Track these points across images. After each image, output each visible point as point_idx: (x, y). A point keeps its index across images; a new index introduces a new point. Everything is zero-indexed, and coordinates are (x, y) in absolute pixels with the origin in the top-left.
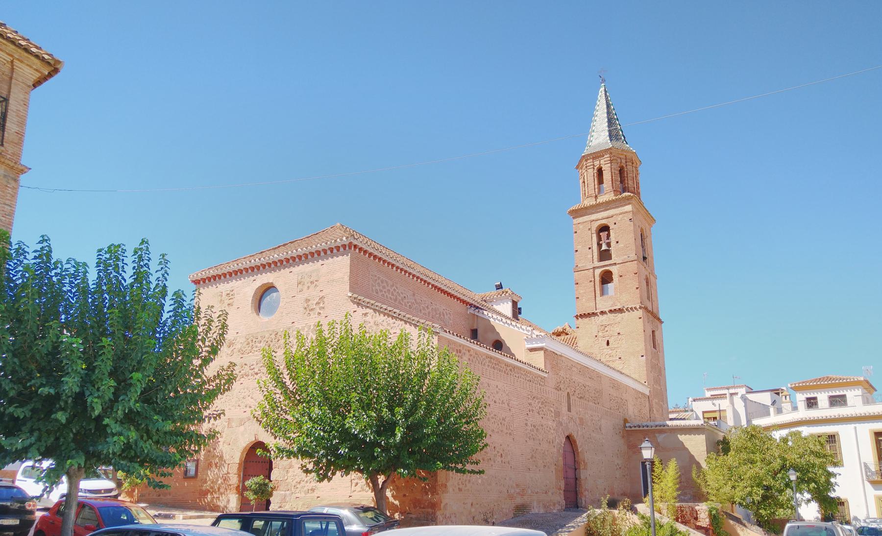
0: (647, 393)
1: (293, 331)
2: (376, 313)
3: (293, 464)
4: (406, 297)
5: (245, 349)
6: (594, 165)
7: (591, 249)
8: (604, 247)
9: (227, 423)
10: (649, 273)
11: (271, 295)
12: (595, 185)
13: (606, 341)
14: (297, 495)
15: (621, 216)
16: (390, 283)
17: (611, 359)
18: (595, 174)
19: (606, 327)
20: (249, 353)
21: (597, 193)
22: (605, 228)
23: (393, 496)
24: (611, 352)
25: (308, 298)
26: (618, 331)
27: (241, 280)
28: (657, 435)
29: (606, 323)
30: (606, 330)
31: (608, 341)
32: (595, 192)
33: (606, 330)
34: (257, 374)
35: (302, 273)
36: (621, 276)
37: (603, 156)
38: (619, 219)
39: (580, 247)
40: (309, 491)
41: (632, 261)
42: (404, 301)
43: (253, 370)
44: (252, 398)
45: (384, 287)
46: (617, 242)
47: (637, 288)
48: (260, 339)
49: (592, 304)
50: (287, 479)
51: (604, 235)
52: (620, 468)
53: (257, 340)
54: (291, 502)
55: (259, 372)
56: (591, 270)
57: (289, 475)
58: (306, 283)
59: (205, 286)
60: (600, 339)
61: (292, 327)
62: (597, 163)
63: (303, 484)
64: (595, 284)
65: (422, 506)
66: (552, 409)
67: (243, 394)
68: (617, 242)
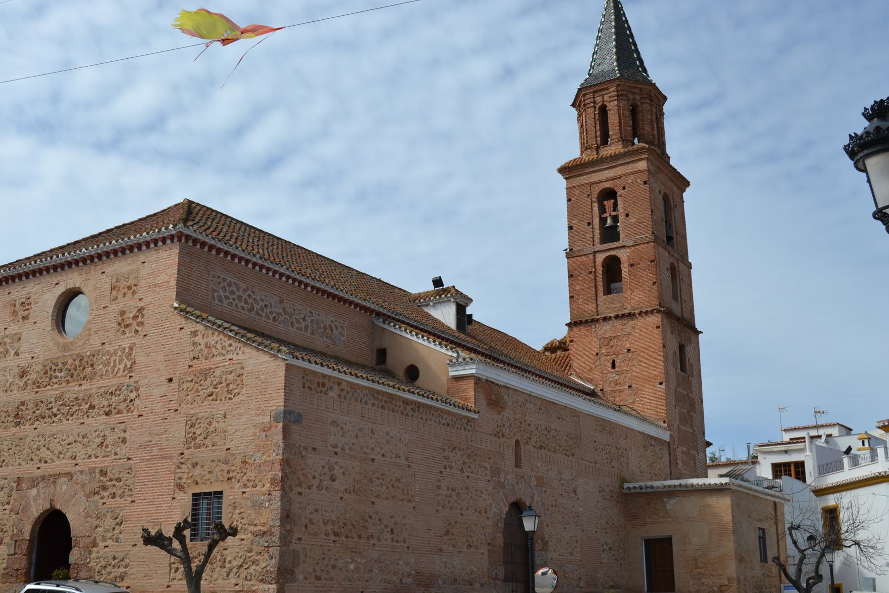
0: (666, 436)
1: (102, 356)
3: (98, 542)
4: (269, 304)
5: (42, 380)
6: (594, 102)
7: (591, 226)
8: (609, 222)
9: (16, 484)
10: (678, 260)
12: (596, 132)
13: (611, 362)
15: (632, 177)
16: (242, 286)
17: (618, 388)
18: (597, 116)
19: (611, 340)
20: (46, 386)
21: (599, 143)
22: (610, 194)
24: (617, 377)
25: (124, 309)
26: (627, 346)
28: (665, 500)
29: (611, 335)
30: (611, 345)
31: (614, 361)
32: (596, 141)
33: (611, 345)
34: (55, 415)
36: (632, 265)
37: (607, 89)
38: (630, 181)
39: (576, 221)
40: (117, 579)
41: (647, 243)
42: (265, 311)
44: (48, 449)
45: (232, 292)
46: (627, 215)
47: (654, 283)
49: (592, 306)
50: (89, 562)
51: (608, 204)
52: (610, 549)
55: (58, 413)
56: (591, 256)
57: (93, 556)
58: (121, 288)
60: (603, 358)
61: (102, 350)
62: (599, 99)
63: (109, 569)
64: (595, 276)
66: (486, 464)
67: (37, 443)
68: (627, 215)
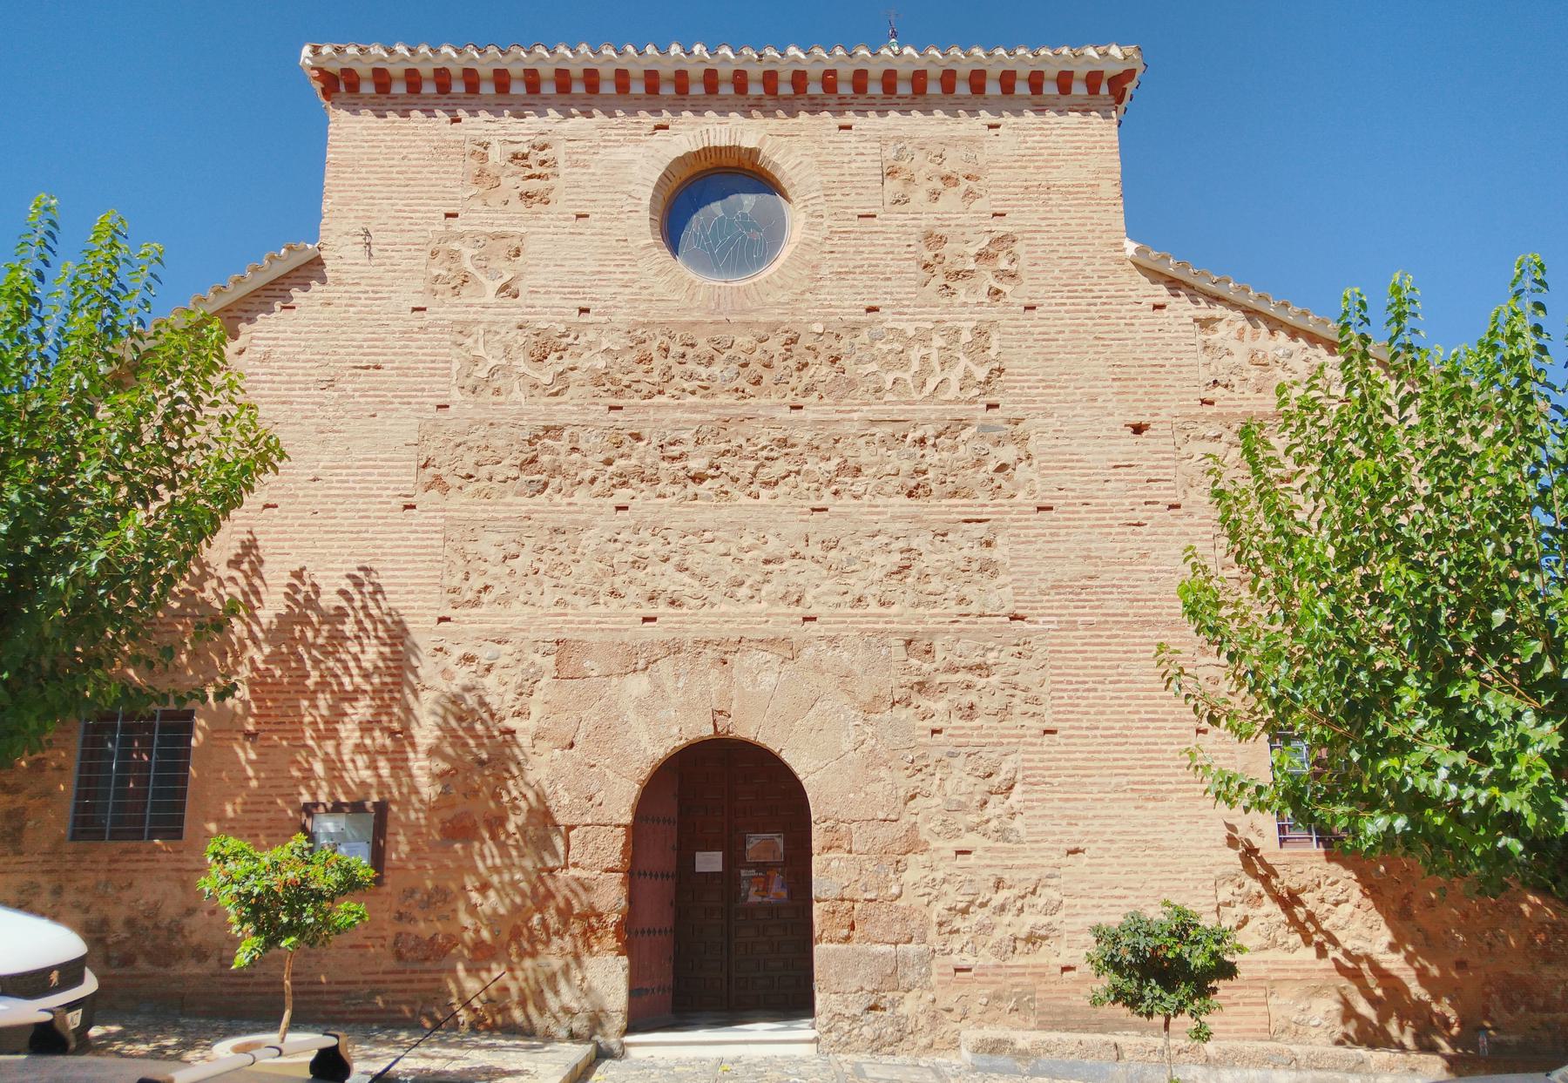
1: (873, 340)
2: (1256, 327)
3: (923, 837)
5: (632, 377)
9: (553, 658)
11: (732, 198)
14: (956, 960)
20: (650, 396)
23: (147, 1043)
25: (939, 231)
27: (589, 115)
34: (698, 478)
35: (899, 139)
40: (1020, 945)
43: (678, 465)
44: (682, 569)
48: (704, 347)
50: (899, 896)
53: (690, 352)
54: (931, 989)
55: (711, 472)
57: (909, 877)
58: (920, 177)
59: (414, 106)
61: (868, 324)
63: (978, 916)
65: (1540, 1002)
67: (633, 549)
